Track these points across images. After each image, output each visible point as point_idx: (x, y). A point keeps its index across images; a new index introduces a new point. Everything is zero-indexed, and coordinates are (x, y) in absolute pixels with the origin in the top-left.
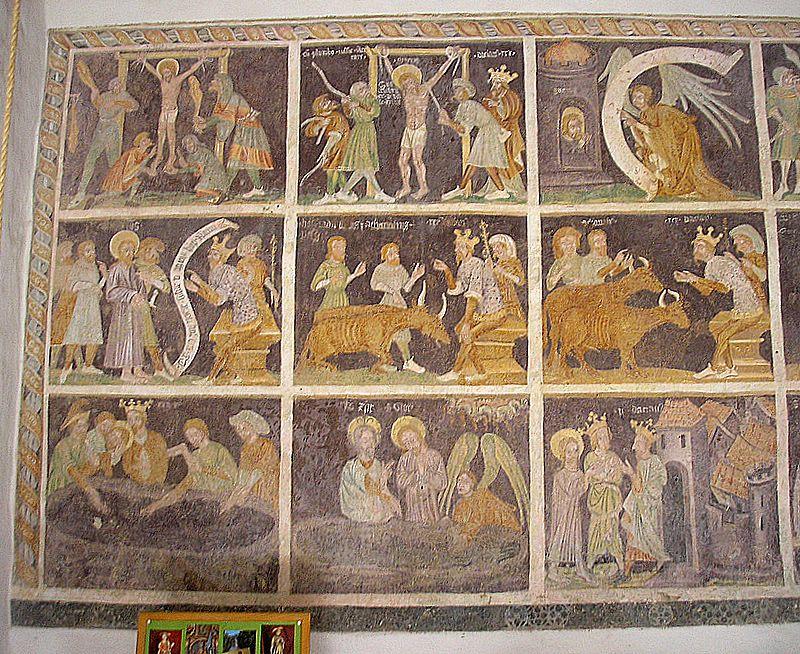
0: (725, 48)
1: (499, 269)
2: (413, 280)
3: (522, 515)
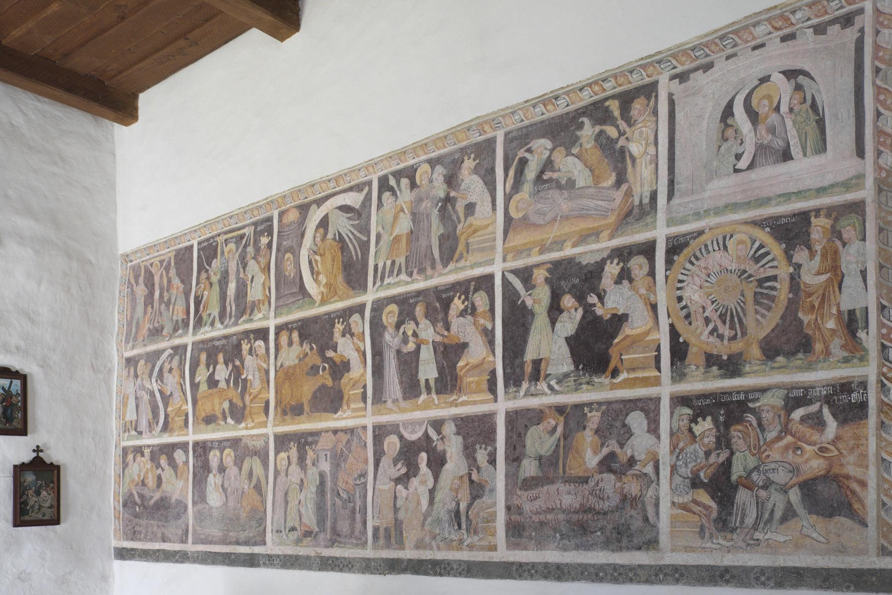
0: (358, 188)
1: (259, 360)
2: (229, 372)
3: (264, 502)
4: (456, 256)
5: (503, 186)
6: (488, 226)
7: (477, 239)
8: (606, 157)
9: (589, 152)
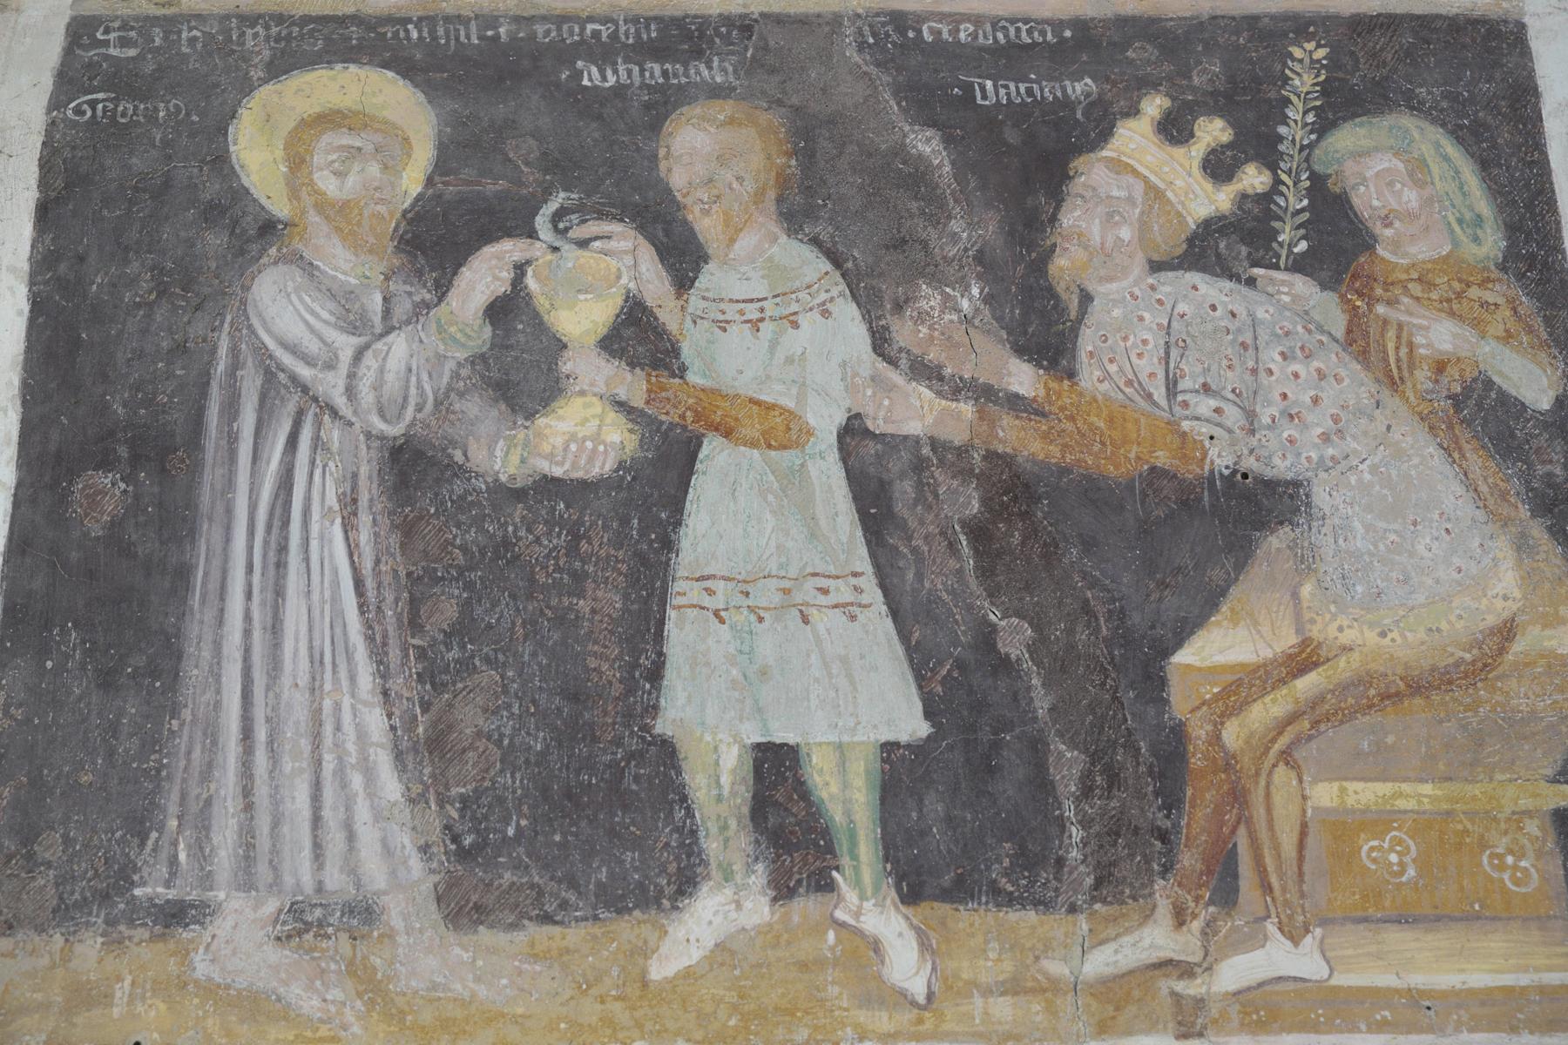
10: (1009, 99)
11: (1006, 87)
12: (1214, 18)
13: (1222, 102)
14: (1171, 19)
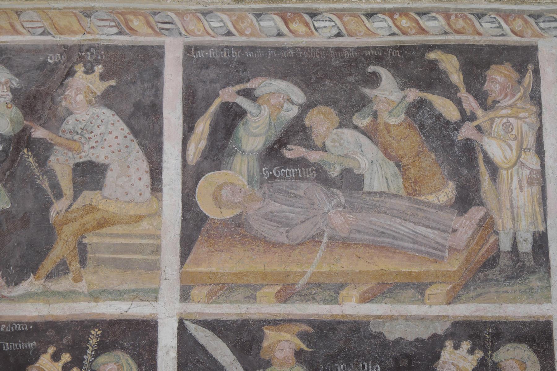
4: (48, 265)
5: (179, 147)
6: (140, 218)
7: (108, 240)
8: (434, 150)
9: (394, 132)
10: (12, 349)
11: (12, 345)
12: (72, 321)
13: (69, 349)
14: (60, 322)
